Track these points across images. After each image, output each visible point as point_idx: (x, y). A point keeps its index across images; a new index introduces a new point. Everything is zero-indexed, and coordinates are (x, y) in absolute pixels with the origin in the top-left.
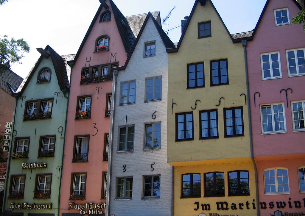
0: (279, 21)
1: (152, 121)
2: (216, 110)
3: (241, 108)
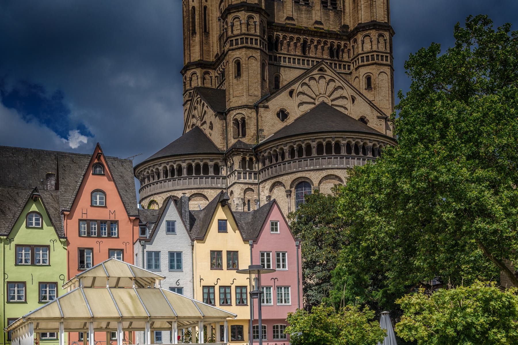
0: (272, 230)
1: (177, 286)
2: (230, 287)
3: (246, 287)
